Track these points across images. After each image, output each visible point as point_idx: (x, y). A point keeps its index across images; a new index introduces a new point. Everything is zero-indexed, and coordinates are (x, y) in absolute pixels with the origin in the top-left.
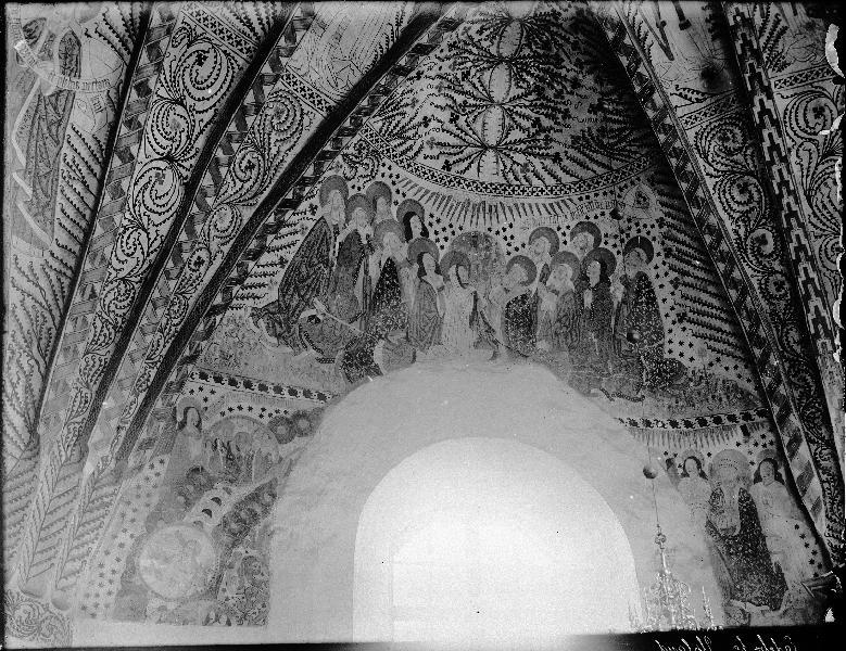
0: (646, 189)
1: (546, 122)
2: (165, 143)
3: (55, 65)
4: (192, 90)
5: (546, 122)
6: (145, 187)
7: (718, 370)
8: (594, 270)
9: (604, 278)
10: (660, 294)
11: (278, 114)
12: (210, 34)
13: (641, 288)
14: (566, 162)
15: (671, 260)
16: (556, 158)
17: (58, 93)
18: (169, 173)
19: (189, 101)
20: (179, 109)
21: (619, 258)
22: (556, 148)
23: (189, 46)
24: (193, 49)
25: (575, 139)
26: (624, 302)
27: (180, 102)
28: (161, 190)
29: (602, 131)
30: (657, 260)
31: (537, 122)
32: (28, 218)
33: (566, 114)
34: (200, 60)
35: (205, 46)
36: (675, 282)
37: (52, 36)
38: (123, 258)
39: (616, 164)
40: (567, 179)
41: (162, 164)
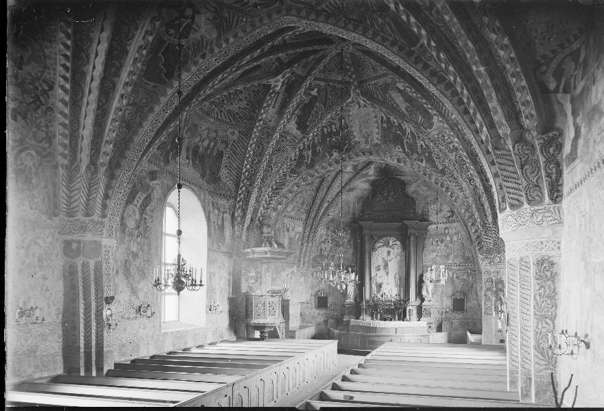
0: (237, 132)
1: (225, 102)
5: (225, 102)
7: (228, 183)
8: (212, 144)
9: (213, 148)
10: (224, 158)
13: (220, 155)
14: (223, 114)
15: (231, 152)
16: (221, 111)
21: (219, 144)
22: (223, 109)
25: (229, 110)
26: (215, 156)
29: (237, 114)
30: (227, 149)
31: (223, 100)
33: (232, 104)
36: (229, 157)
39: (233, 122)
40: (220, 117)
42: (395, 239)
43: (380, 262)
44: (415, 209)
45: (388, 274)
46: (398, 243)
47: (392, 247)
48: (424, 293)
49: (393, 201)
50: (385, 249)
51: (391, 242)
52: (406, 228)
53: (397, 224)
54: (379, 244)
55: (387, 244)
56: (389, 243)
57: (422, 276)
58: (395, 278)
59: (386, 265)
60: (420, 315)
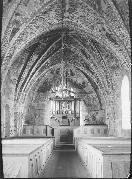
2: (117, 27)
3: (104, 32)
4: (115, 18)
6: (119, 33)
11: (124, 8)
12: (109, 13)
17: (106, 33)
18: (120, 29)
19: (116, 19)
20: (116, 21)
23: (109, 16)
24: (110, 15)
27: (115, 21)
28: (121, 31)
32: (116, 46)
34: (112, 15)
35: (110, 14)
37: (101, 30)
38: (125, 41)
41: (119, 29)
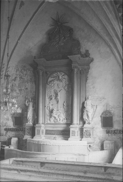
42: (63, 74)
43: (53, 94)
44: (79, 49)
45: (58, 102)
46: (66, 77)
47: (61, 81)
48: (85, 117)
49: (62, 44)
50: (56, 82)
51: (60, 76)
52: (71, 62)
53: (64, 61)
54: (52, 79)
55: (59, 79)
56: (59, 77)
57: (83, 103)
58: (64, 105)
59: (57, 95)
60: (82, 135)
